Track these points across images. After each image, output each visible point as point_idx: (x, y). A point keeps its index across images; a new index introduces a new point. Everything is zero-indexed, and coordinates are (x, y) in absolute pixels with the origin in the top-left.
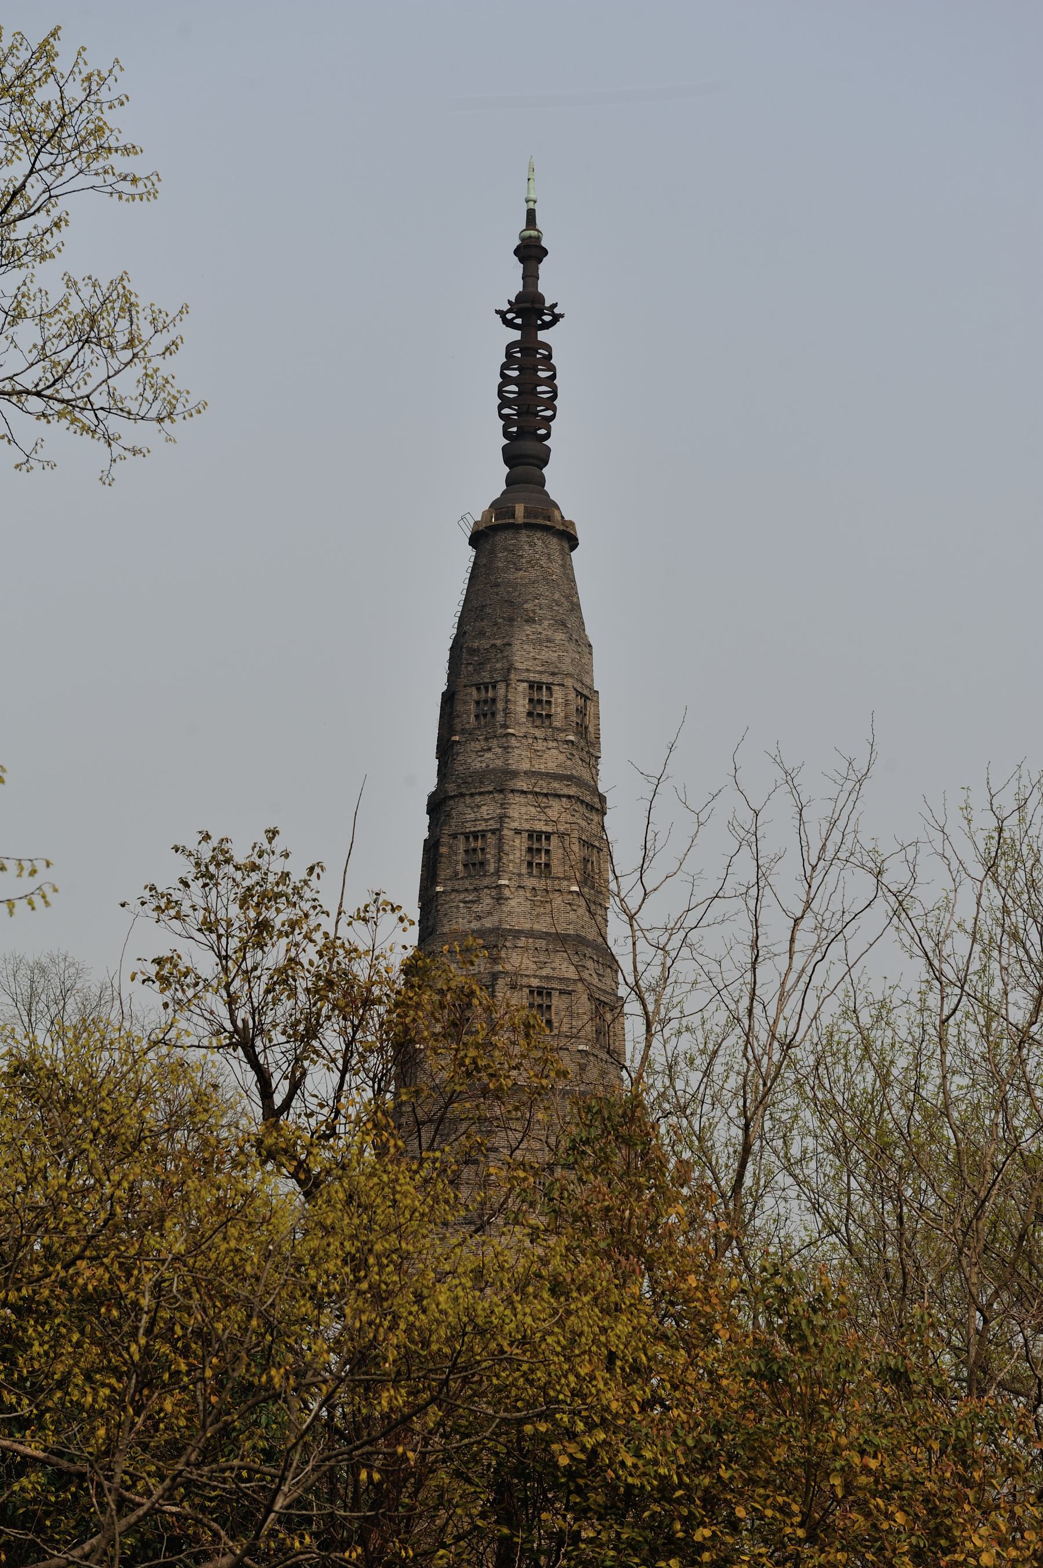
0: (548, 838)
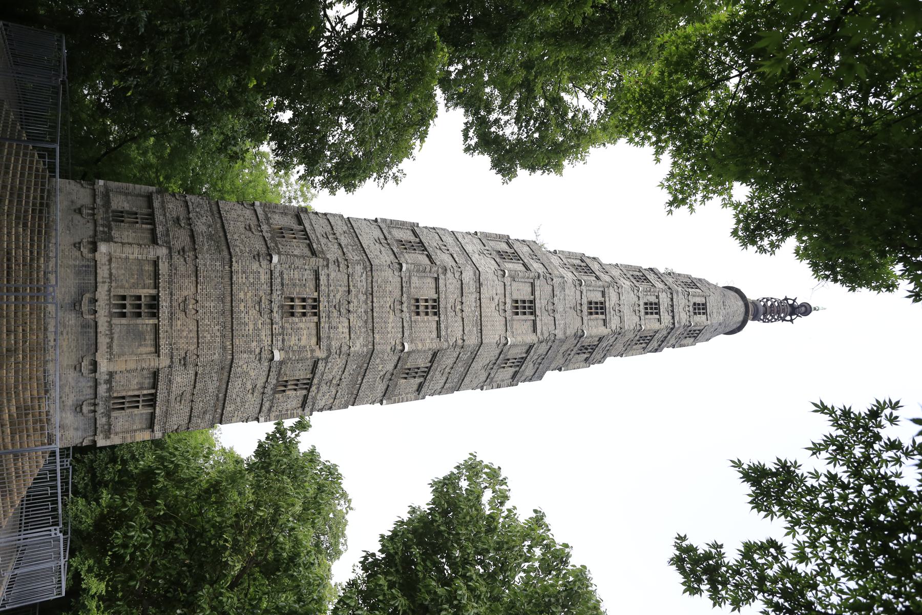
0: (656, 313)
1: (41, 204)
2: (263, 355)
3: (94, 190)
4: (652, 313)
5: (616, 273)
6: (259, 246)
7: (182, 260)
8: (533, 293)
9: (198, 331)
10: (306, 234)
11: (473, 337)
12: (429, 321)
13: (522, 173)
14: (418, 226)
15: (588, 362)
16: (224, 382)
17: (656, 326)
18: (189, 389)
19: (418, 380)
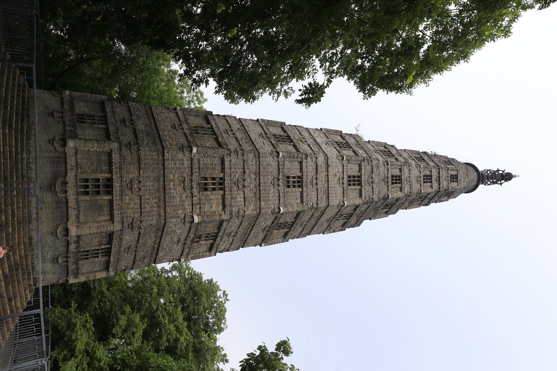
0: (430, 182)
1: (23, 109)
2: (187, 220)
3: (62, 98)
4: (427, 182)
5: (406, 155)
6: (182, 140)
7: (129, 152)
8: (360, 171)
9: (141, 204)
10: (213, 131)
11: (324, 202)
12: (296, 192)
13: (381, 93)
14: (285, 124)
15: (387, 214)
16: (159, 237)
17: (429, 190)
18: (134, 244)
19: (285, 230)
